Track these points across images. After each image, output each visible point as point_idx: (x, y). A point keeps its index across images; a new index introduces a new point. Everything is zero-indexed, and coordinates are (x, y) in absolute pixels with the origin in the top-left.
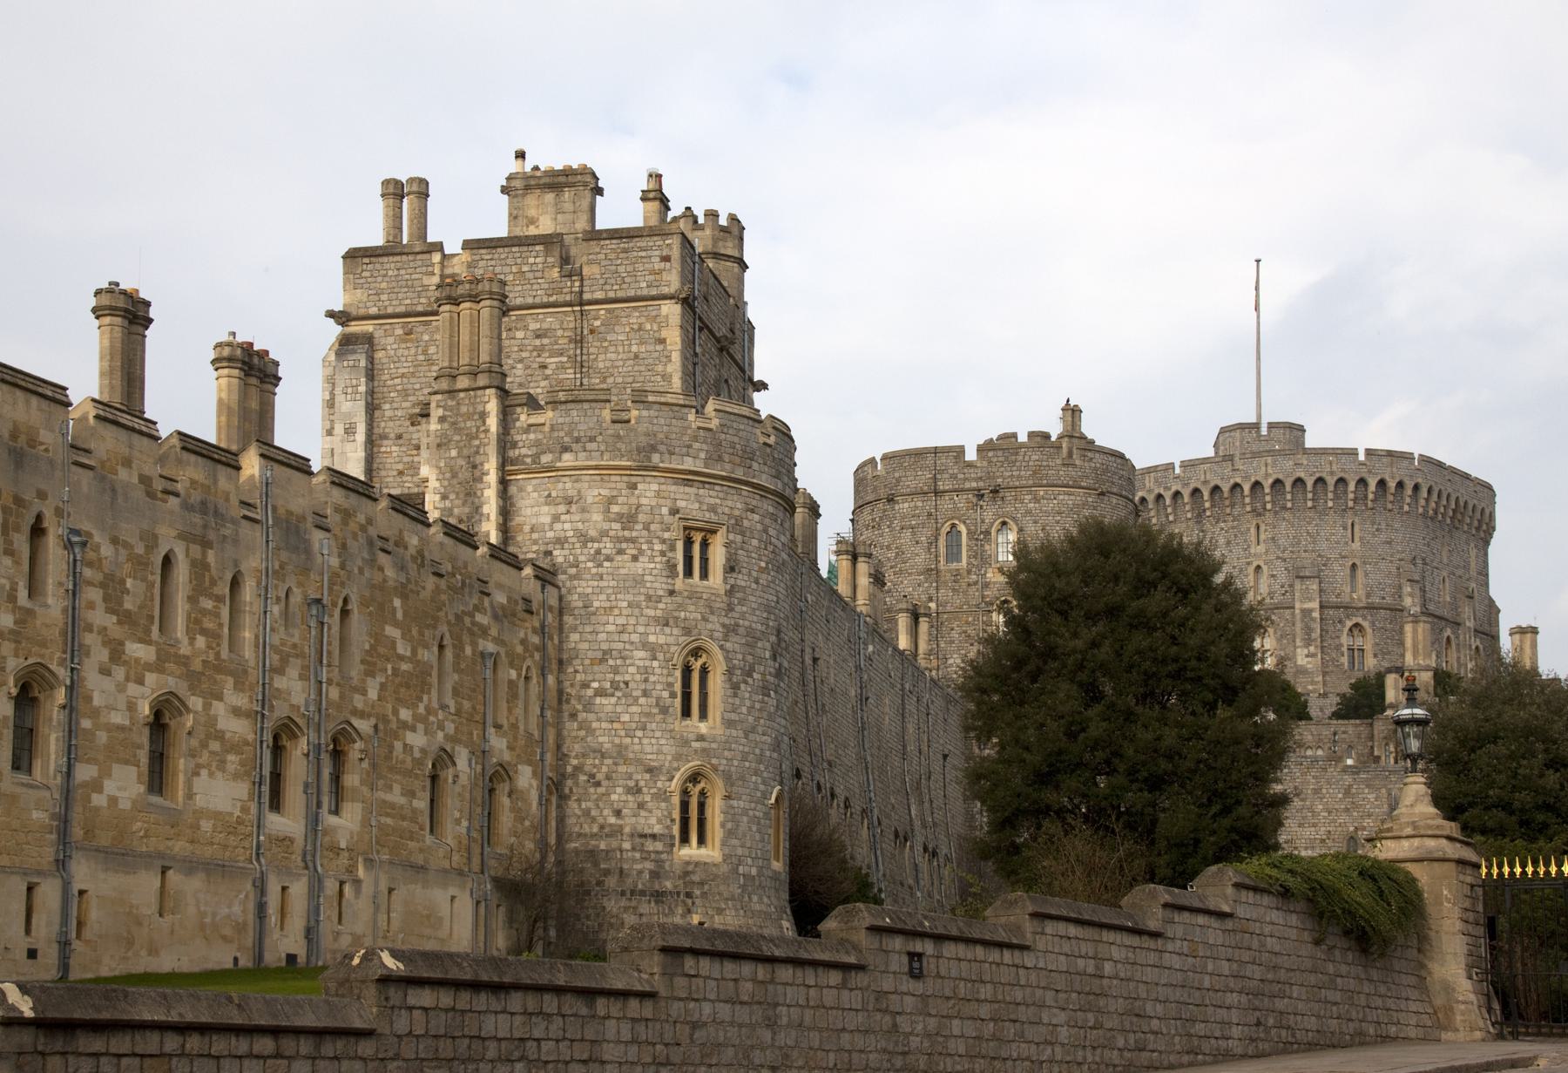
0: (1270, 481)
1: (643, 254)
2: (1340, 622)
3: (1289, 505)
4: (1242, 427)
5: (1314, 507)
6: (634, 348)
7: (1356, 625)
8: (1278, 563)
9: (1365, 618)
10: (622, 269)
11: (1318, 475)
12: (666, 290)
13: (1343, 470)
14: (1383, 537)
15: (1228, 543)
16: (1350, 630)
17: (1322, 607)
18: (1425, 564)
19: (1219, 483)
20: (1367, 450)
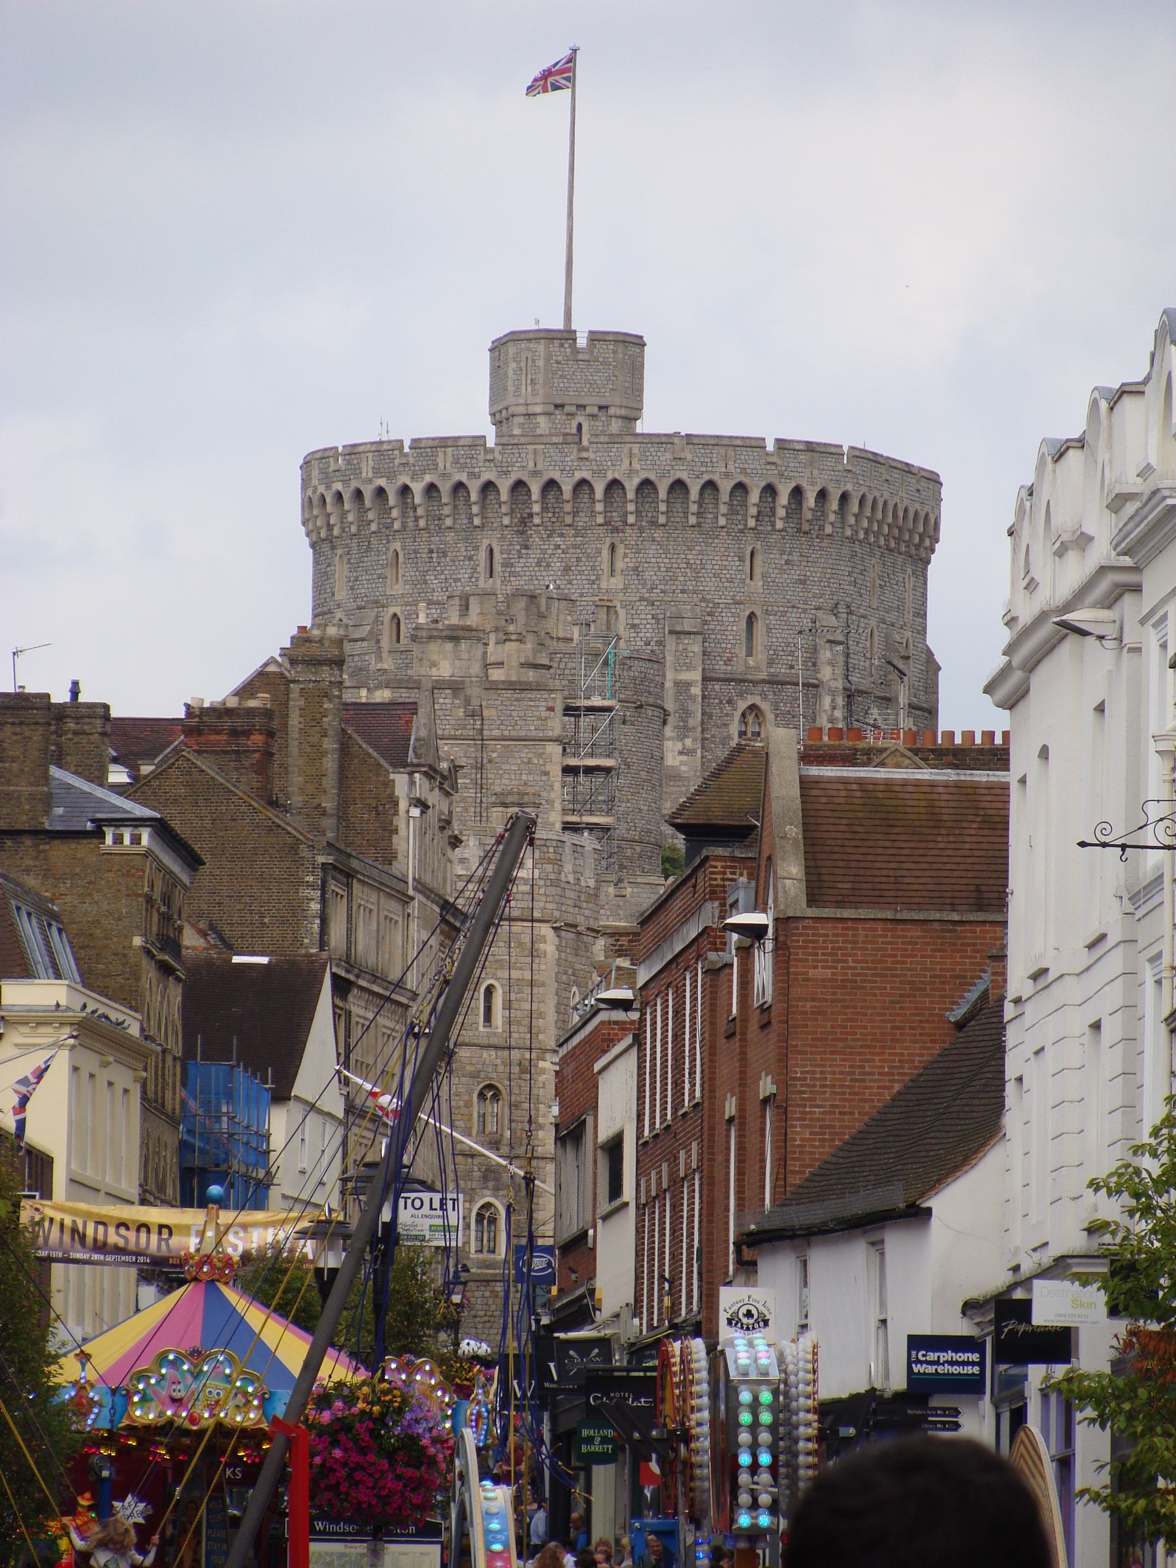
0: (636, 481)
1: (532, 703)
2: (729, 702)
3: (662, 520)
4: (549, 336)
5: (699, 525)
6: (524, 777)
7: (753, 707)
8: (642, 606)
9: (764, 697)
10: (515, 714)
11: (706, 477)
12: (550, 734)
13: (744, 471)
14: (795, 574)
15: (567, 569)
16: (743, 715)
17: (705, 679)
18: (850, 613)
19: (556, 475)
20: (778, 441)
